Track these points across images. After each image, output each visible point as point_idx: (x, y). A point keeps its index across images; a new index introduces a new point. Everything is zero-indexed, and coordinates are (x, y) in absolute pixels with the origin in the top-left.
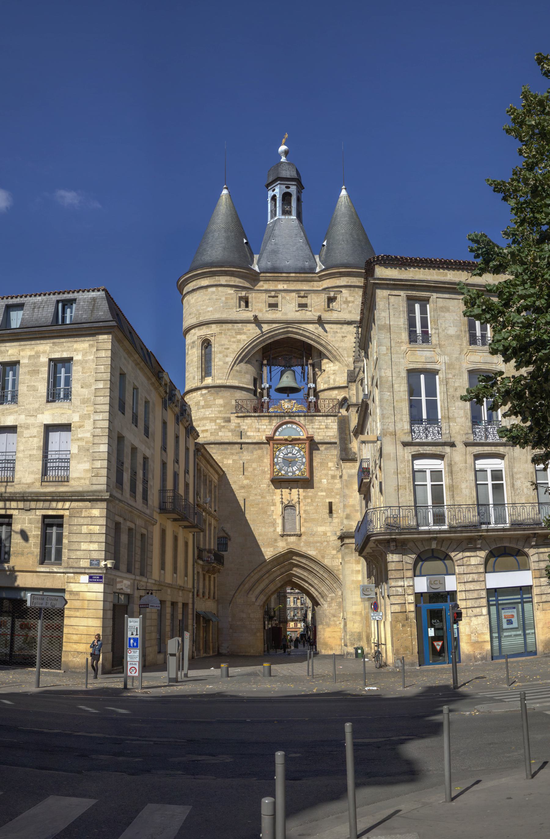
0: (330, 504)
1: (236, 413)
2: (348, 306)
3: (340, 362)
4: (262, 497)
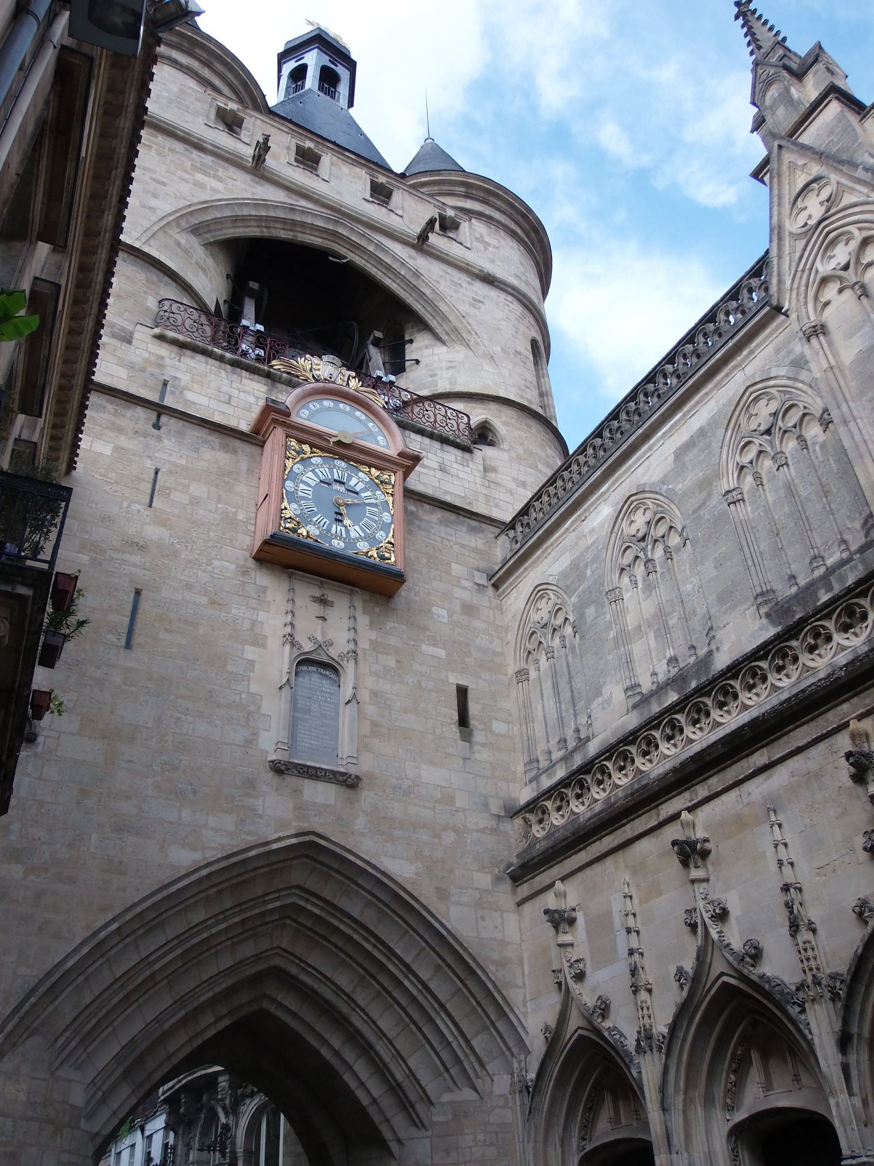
0: (462, 693)
1: (157, 326)
2: (486, 249)
3: (468, 346)
4: (213, 602)
